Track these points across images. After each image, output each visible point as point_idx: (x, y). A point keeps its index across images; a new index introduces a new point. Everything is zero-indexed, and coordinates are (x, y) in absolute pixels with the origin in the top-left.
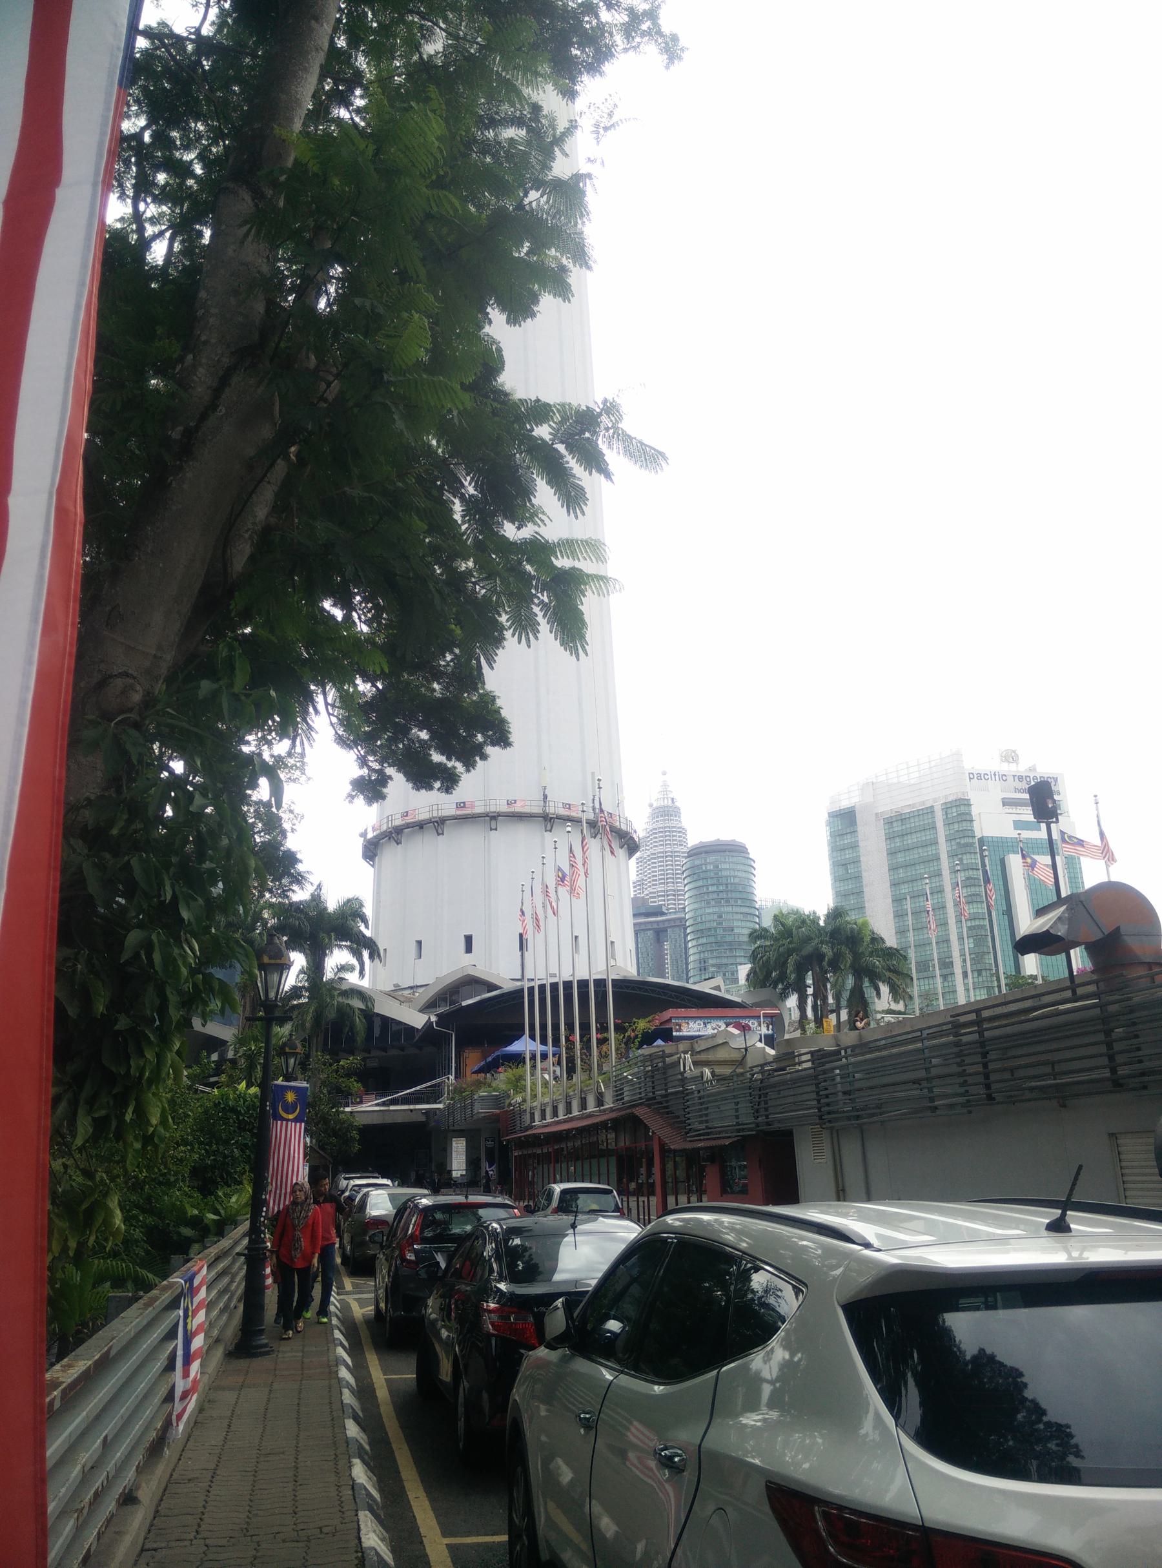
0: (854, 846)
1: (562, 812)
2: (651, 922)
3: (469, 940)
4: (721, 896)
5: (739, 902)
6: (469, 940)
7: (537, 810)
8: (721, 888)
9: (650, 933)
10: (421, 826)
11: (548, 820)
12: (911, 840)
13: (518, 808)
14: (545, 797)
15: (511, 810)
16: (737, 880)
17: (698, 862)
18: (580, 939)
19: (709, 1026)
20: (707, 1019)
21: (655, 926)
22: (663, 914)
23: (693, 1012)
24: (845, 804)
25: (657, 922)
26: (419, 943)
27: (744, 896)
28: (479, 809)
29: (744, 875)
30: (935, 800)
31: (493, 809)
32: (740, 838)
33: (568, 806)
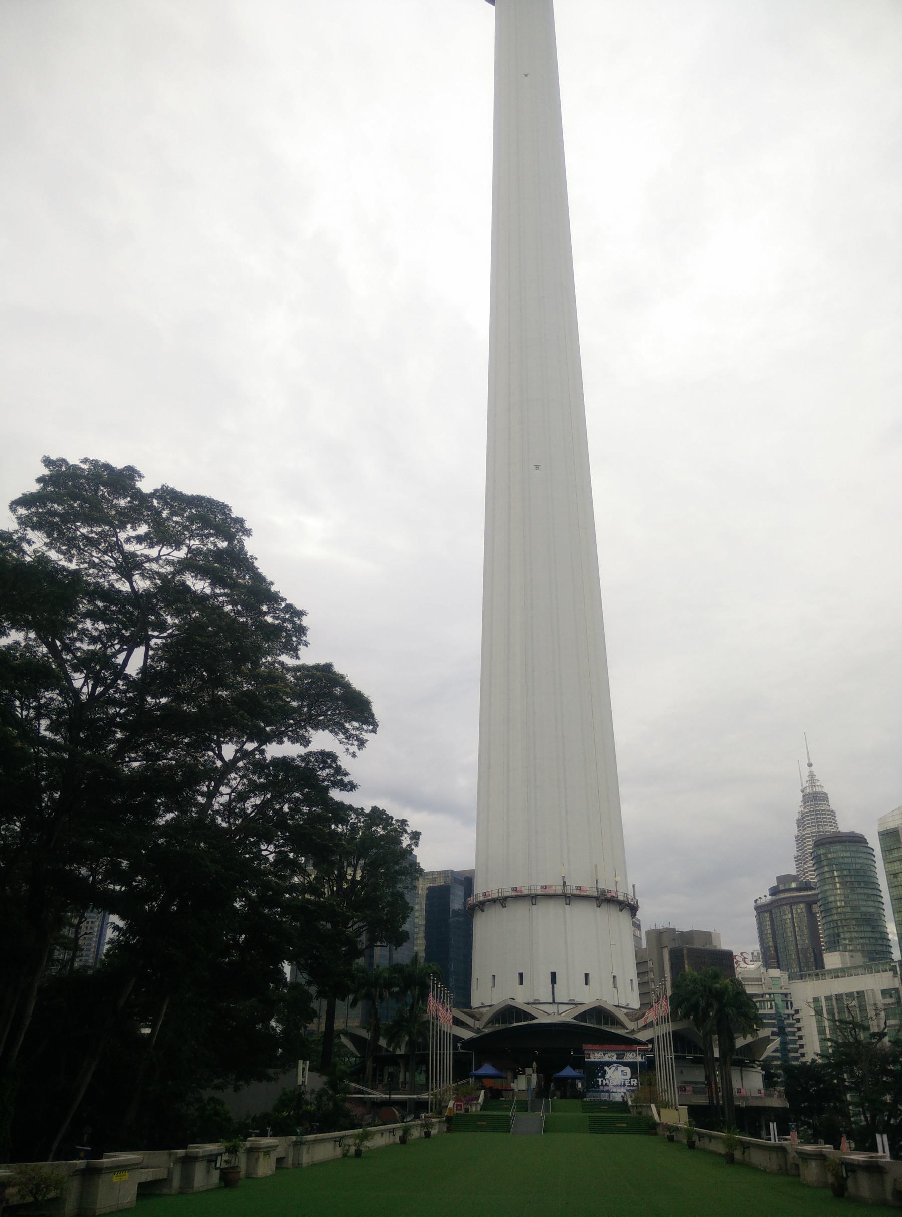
1: (575, 892)
3: (521, 975)
4: (848, 879)
5: (862, 885)
6: (521, 975)
7: (560, 892)
8: (845, 873)
10: (494, 901)
11: (568, 898)
13: (548, 891)
14: (565, 883)
17: (822, 851)
20: (605, 1052)
21: (807, 899)
22: (812, 889)
23: (597, 1046)
24: (891, 825)
25: (808, 896)
26: (494, 976)
27: (867, 879)
28: (525, 892)
29: (865, 861)
32: (858, 830)
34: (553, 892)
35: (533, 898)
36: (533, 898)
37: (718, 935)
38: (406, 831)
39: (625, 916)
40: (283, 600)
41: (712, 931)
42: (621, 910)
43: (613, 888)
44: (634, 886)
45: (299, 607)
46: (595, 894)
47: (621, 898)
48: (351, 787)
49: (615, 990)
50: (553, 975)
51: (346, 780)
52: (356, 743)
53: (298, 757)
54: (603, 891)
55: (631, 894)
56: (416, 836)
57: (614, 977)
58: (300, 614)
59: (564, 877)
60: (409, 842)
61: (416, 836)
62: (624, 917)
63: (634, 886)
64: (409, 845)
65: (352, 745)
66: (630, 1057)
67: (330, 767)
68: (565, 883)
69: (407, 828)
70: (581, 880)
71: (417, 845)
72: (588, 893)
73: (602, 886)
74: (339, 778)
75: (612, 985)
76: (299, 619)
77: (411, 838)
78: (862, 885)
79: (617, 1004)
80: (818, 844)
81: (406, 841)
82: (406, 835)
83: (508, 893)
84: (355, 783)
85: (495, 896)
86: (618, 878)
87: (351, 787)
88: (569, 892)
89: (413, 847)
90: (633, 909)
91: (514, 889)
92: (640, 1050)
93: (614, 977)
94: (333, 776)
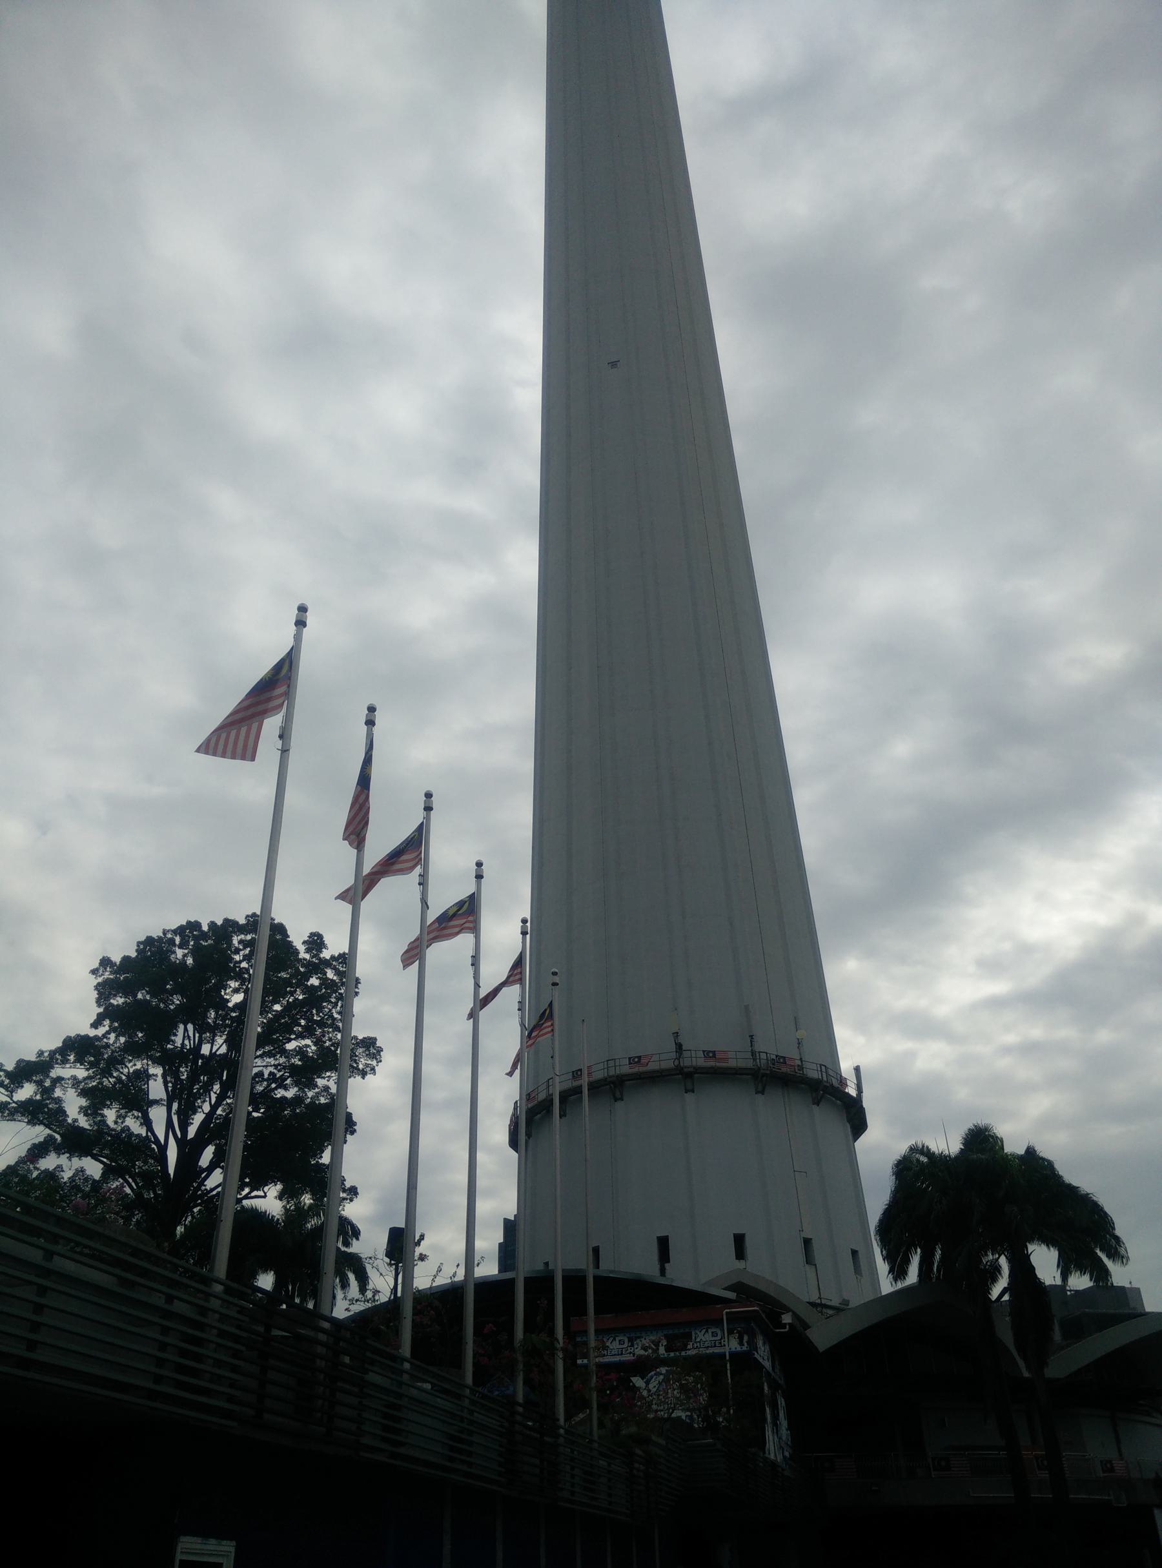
1: (701, 1062)
7: (668, 1064)
14: (679, 1047)
15: (636, 1070)
18: (815, 1245)
19: (639, 1344)
31: (612, 1073)
33: (710, 1054)
37: (1138, 1290)
39: (828, 1121)
41: (1127, 1285)
43: (792, 1053)
44: (857, 1070)
47: (813, 1074)
49: (810, 1270)
50: (663, 1244)
57: (807, 1242)
59: (676, 1034)
63: (857, 1070)
66: (704, 1341)
68: (679, 1047)
70: (714, 1034)
72: (732, 1063)
75: (802, 1258)
79: (814, 1298)
86: (801, 1034)
92: (732, 1318)
93: (807, 1242)
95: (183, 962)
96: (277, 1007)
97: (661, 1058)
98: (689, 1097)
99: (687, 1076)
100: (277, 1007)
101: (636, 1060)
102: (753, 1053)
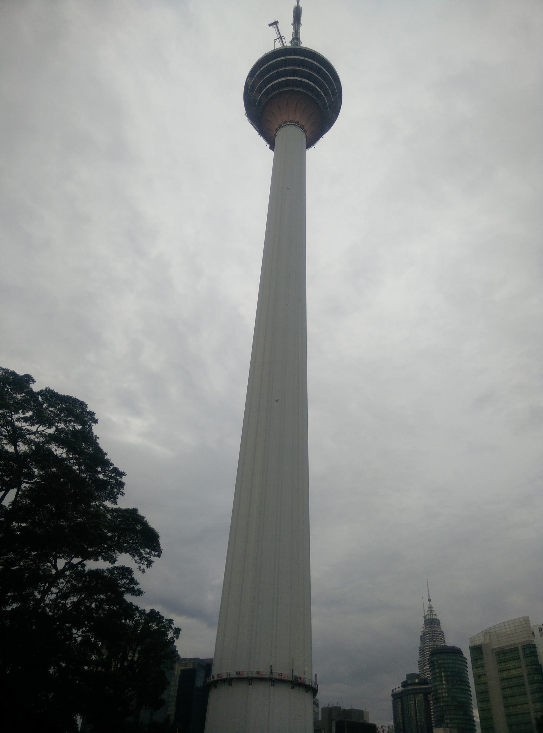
0: (483, 666)
1: (278, 677)
2: (421, 688)
5: (459, 682)
8: (449, 674)
9: (421, 695)
10: (224, 681)
11: (274, 681)
12: (509, 665)
13: (259, 676)
14: (272, 670)
16: (457, 670)
17: (435, 659)
22: (428, 684)
24: (477, 643)
25: (425, 688)
28: (245, 675)
30: (519, 643)
31: (250, 675)
33: (281, 674)
34: (264, 676)
35: (250, 680)
36: (250, 680)
38: (171, 628)
40: (112, 465)
41: (364, 710)
42: (307, 692)
43: (302, 676)
44: (316, 675)
45: (121, 470)
46: (291, 679)
48: (139, 593)
51: (136, 587)
52: (146, 563)
53: (107, 569)
54: (296, 677)
55: (314, 680)
56: (177, 631)
58: (122, 474)
59: (271, 666)
60: (172, 636)
61: (177, 631)
62: (307, 697)
63: (316, 675)
64: (172, 638)
65: (143, 564)
67: (127, 578)
68: (272, 670)
69: (172, 625)
70: (282, 670)
71: (177, 638)
72: (286, 678)
73: (296, 673)
74: (132, 586)
76: (121, 478)
77: (174, 633)
78: (459, 682)
80: (433, 654)
81: (170, 634)
82: (171, 631)
83: (234, 675)
84: (142, 590)
85: (225, 677)
86: (306, 669)
87: (139, 593)
88: (273, 676)
89: (175, 639)
90: (313, 691)
91: (238, 673)
94: (128, 584)
95: (12, 524)
96: (102, 596)
97: (265, 672)
98: (272, 687)
99: (274, 681)
100: (102, 596)
101: (258, 673)
102: (292, 675)
